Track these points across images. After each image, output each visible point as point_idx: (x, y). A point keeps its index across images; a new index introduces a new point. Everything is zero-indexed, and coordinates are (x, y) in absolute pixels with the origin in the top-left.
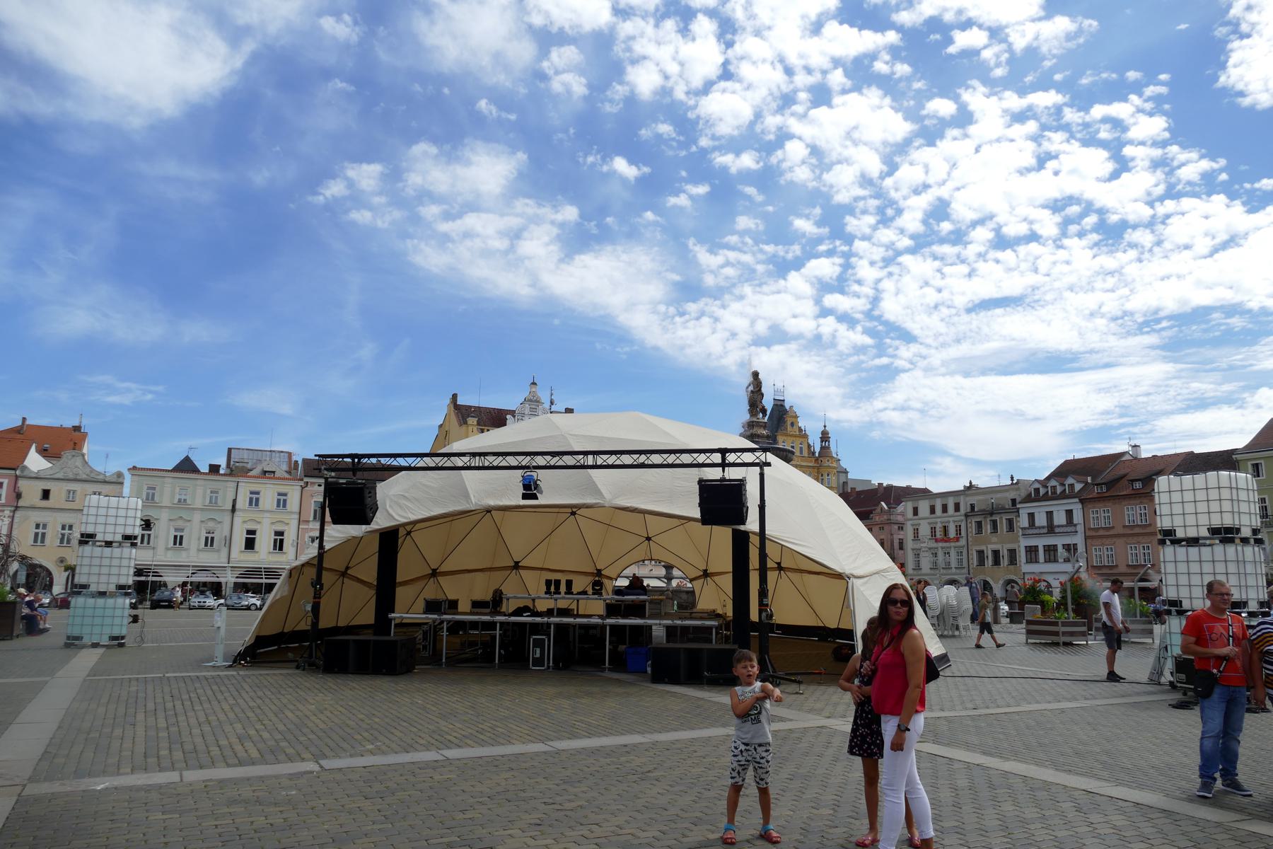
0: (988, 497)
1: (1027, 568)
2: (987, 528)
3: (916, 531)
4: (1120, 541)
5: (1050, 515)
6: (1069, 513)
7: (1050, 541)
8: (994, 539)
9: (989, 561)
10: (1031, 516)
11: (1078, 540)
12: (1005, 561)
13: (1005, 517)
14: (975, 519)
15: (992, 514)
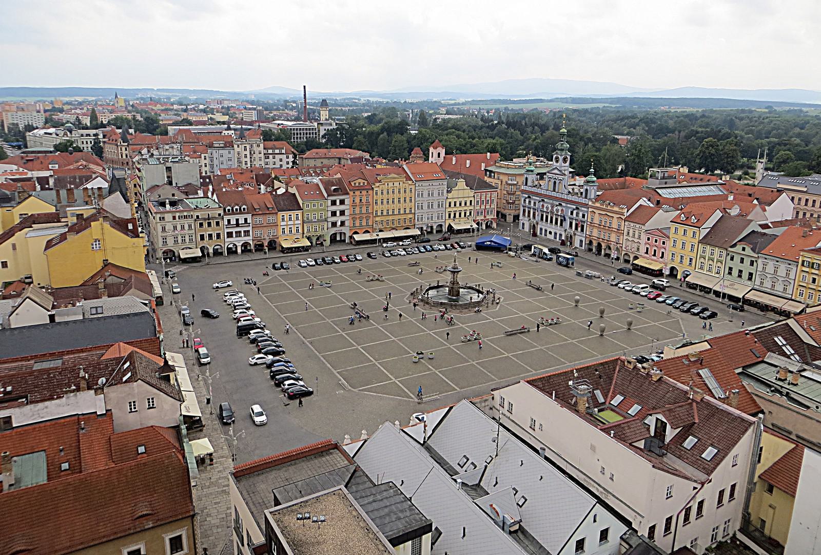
0: (207, 212)
1: (227, 240)
2: (205, 225)
3: (164, 229)
4: (265, 228)
5: (237, 220)
6: (246, 220)
7: (238, 229)
8: (210, 229)
9: (206, 238)
10: (229, 221)
11: (250, 228)
12: (214, 238)
13: (215, 221)
14: (199, 222)
15: (209, 219)
